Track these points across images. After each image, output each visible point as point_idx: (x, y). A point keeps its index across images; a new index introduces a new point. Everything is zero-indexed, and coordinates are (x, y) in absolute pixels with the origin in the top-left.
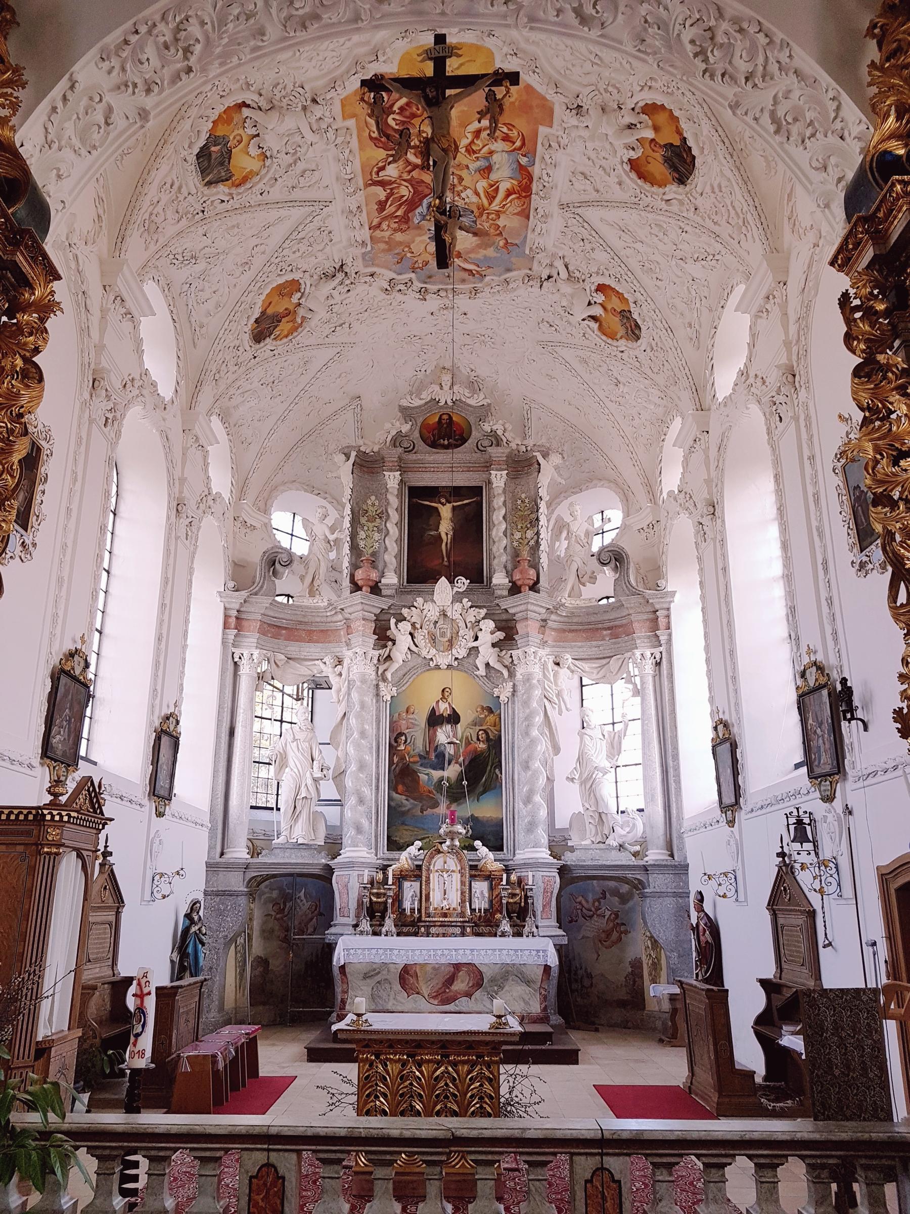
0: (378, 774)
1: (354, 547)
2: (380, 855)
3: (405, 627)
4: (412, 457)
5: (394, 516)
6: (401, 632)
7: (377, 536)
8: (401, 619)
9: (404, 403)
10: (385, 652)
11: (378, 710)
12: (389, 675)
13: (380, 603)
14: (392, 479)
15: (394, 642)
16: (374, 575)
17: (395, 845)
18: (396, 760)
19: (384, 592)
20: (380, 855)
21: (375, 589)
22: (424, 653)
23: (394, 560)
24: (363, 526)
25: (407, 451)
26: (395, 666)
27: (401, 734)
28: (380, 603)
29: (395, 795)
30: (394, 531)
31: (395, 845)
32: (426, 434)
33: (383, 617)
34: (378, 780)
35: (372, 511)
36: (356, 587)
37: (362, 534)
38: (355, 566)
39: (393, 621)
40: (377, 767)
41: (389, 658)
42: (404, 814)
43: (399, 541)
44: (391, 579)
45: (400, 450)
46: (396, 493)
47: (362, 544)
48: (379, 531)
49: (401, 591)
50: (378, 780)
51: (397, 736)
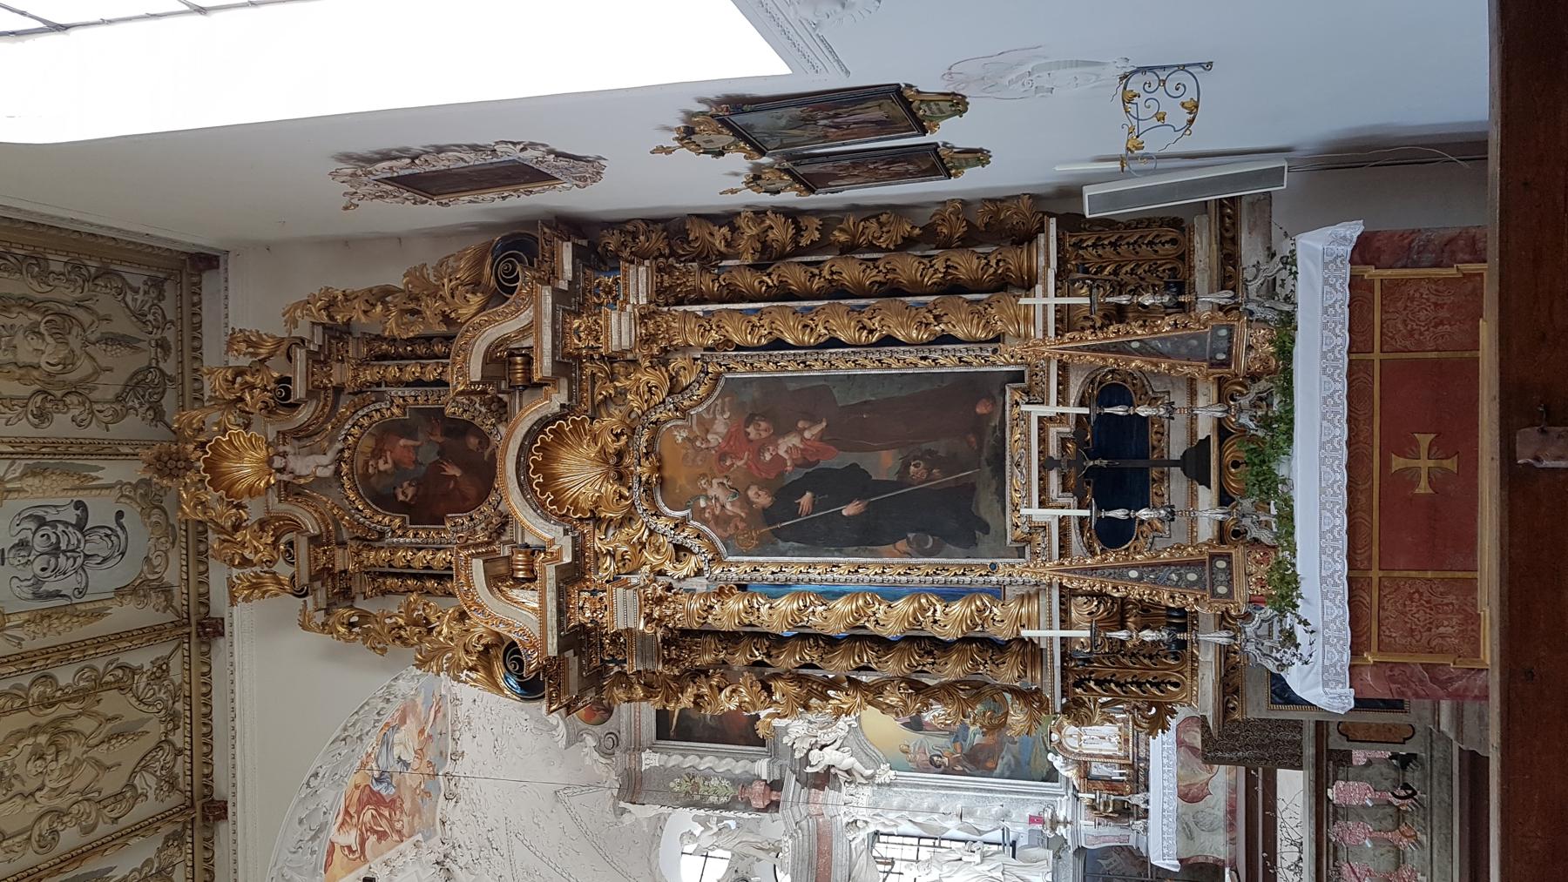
0: (975, 789)
1: (726, 807)
2: (1062, 792)
3: (815, 755)
4: (623, 736)
5: (692, 760)
6: (820, 760)
7: (715, 782)
8: (806, 761)
9: (562, 743)
10: (842, 776)
11: (905, 785)
12: (869, 772)
13: (791, 783)
14: (650, 760)
15: (830, 767)
16: (758, 787)
17: (1051, 775)
18: (959, 768)
19: (777, 777)
20: (1062, 792)
21: (776, 785)
22: (843, 733)
23: (741, 763)
24: (703, 797)
25: (616, 744)
26: (858, 766)
27: (932, 761)
28: (791, 783)
29: (998, 771)
30: (707, 763)
31: (1051, 775)
32: (597, 718)
33: (804, 778)
34: (981, 790)
35: (686, 787)
36: (774, 806)
37: (713, 799)
38: (747, 806)
39: (809, 770)
40: (967, 789)
41: (848, 772)
42: (1018, 762)
43: (720, 756)
44: (762, 768)
45: (617, 753)
46: (665, 757)
47: (724, 799)
48: (707, 778)
49: (774, 755)
50: (981, 790)
51: (934, 766)
